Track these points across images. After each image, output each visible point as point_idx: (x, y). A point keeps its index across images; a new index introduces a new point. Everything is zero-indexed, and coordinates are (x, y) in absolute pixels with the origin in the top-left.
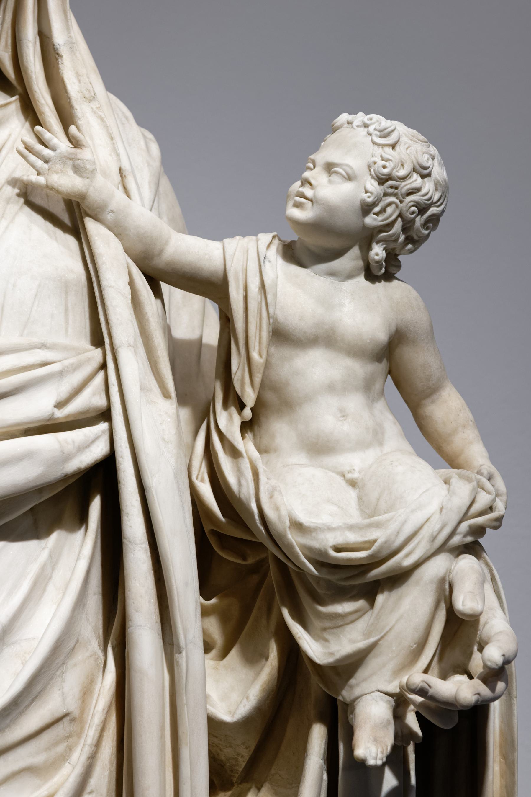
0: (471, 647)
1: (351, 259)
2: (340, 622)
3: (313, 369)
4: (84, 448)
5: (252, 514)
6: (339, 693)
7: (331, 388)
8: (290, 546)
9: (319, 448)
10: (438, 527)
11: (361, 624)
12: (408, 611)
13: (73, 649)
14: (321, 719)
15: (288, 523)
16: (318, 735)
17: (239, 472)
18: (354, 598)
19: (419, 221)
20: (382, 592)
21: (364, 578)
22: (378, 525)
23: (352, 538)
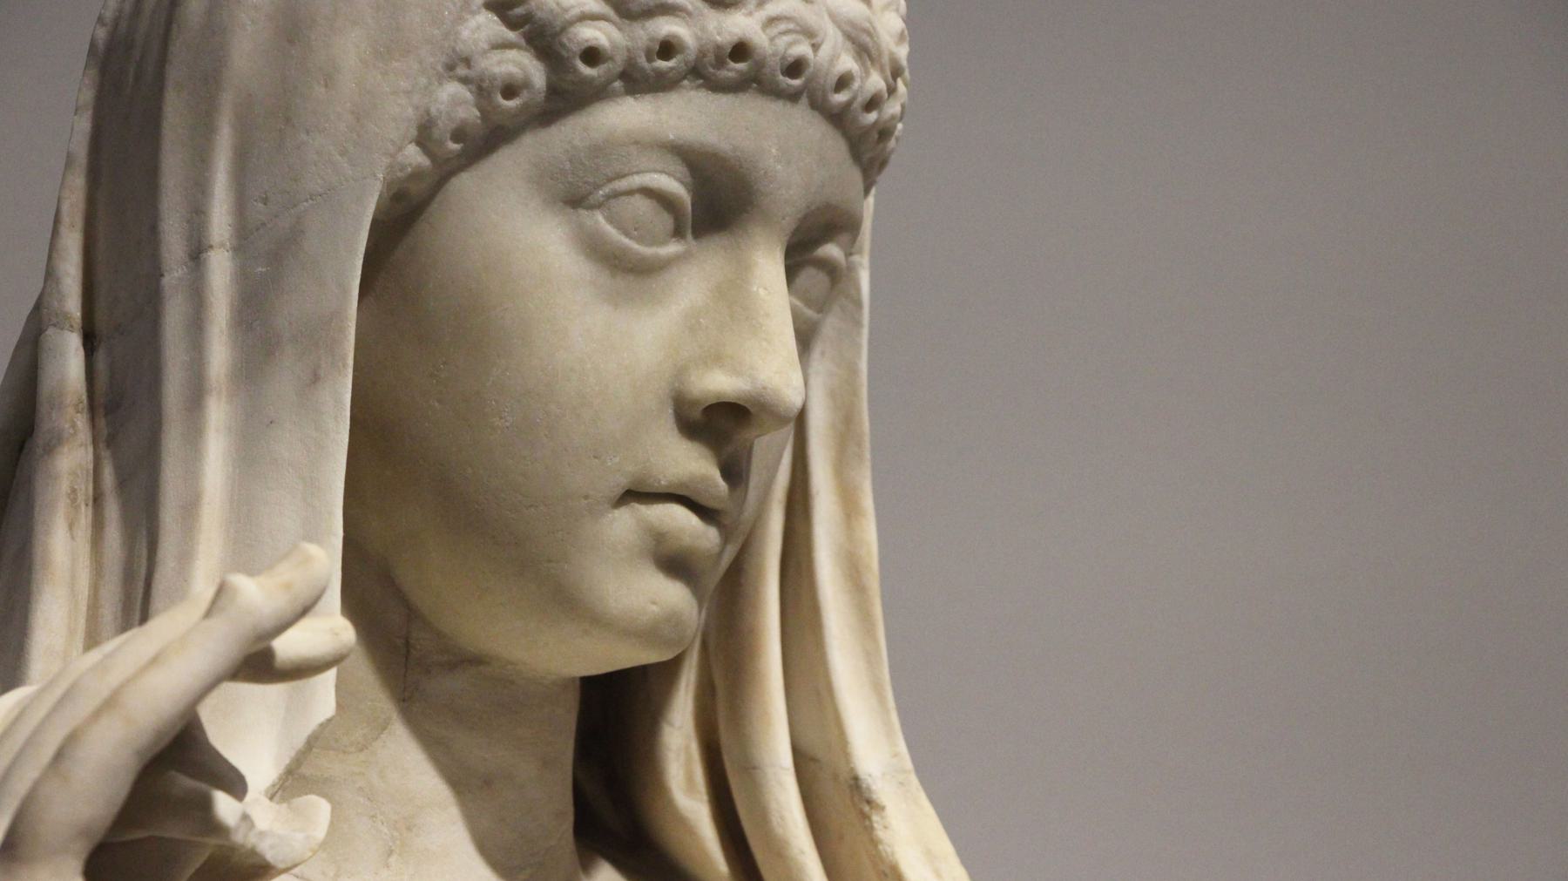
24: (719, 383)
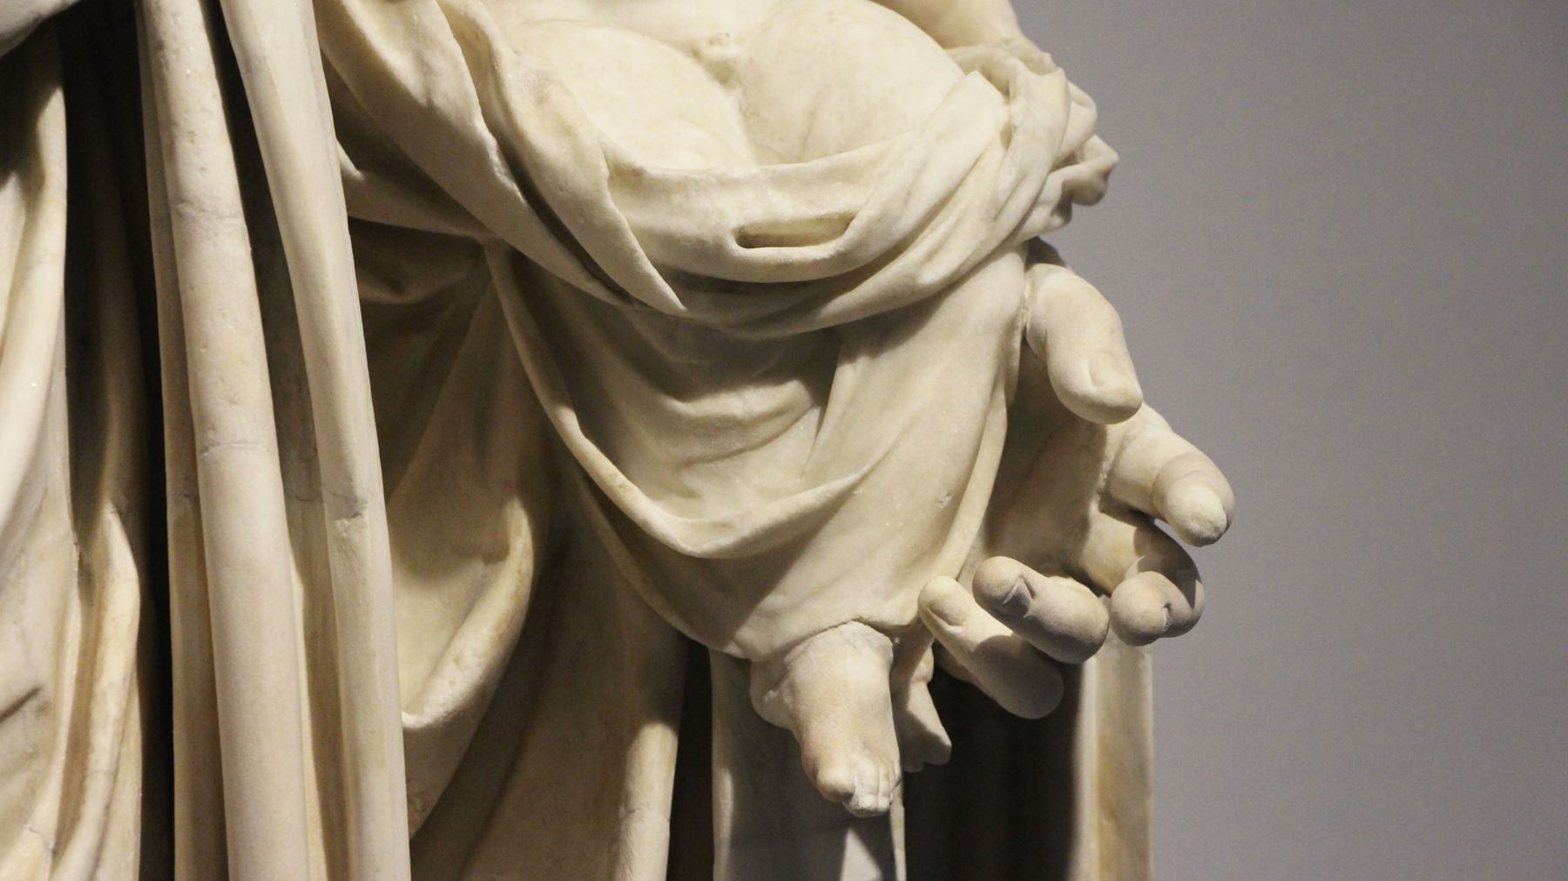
0: (1081, 502)
2: (734, 439)
5: (479, 152)
6: (727, 635)
8: (611, 233)
10: (1007, 181)
11: (795, 445)
13: (39, 511)
14: (666, 718)
15: (605, 171)
16: (655, 755)
17: (416, 37)
18: (775, 376)
20: (851, 357)
21: (796, 322)
22: (848, 175)
23: (786, 207)
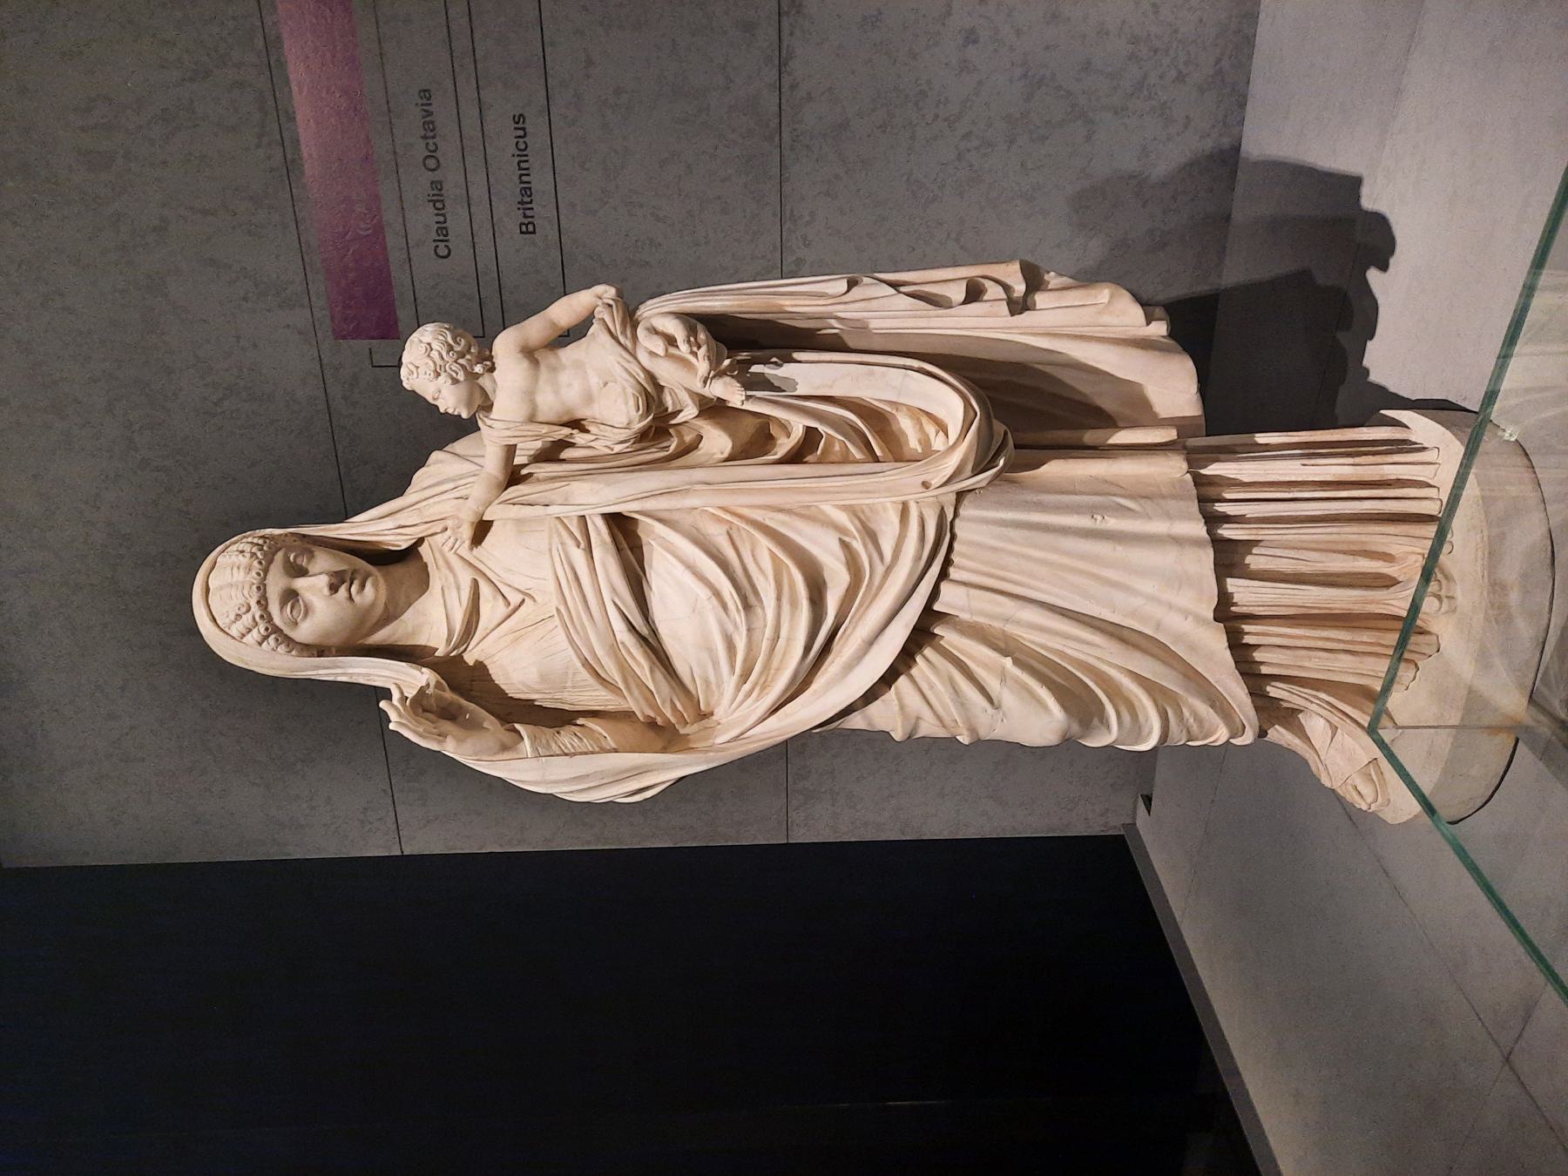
1: (485, 382)
3: (548, 403)
4: (600, 532)
7: (556, 392)
9: (589, 399)
12: (667, 373)
19: (458, 348)
23: (632, 402)
24: (326, 591)
